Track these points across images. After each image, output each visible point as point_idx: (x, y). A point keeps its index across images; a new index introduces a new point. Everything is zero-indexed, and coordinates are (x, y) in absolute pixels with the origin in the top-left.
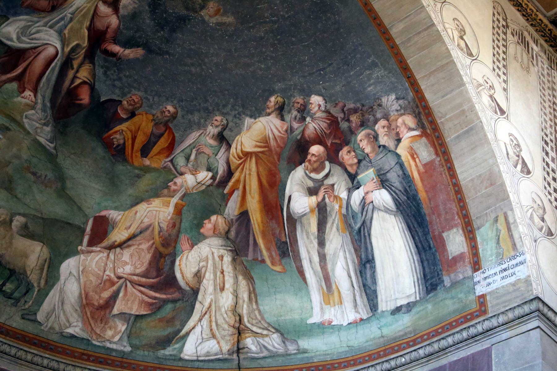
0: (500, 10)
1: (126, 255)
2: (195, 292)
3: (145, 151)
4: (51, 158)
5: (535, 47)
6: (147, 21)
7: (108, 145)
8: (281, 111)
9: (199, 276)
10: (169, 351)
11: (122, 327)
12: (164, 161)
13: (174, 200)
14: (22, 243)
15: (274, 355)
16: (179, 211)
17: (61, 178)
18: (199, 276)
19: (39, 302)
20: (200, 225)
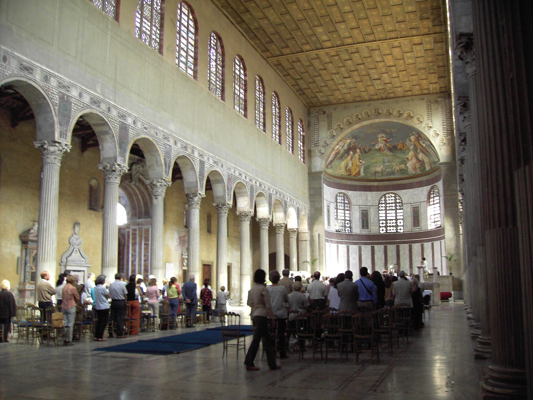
0: (429, 101)
1: (413, 160)
2: (423, 161)
3: (404, 147)
4: (395, 156)
5: (440, 99)
6: (388, 136)
7: (399, 150)
8: (412, 135)
9: (422, 158)
10: (425, 171)
11: (419, 169)
12: (406, 147)
13: (412, 151)
14: (401, 166)
15: (434, 167)
16: (413, 152)
17: (397, 157)
18: (422, 158)
19: (408, 171)
20: (417, 152)
